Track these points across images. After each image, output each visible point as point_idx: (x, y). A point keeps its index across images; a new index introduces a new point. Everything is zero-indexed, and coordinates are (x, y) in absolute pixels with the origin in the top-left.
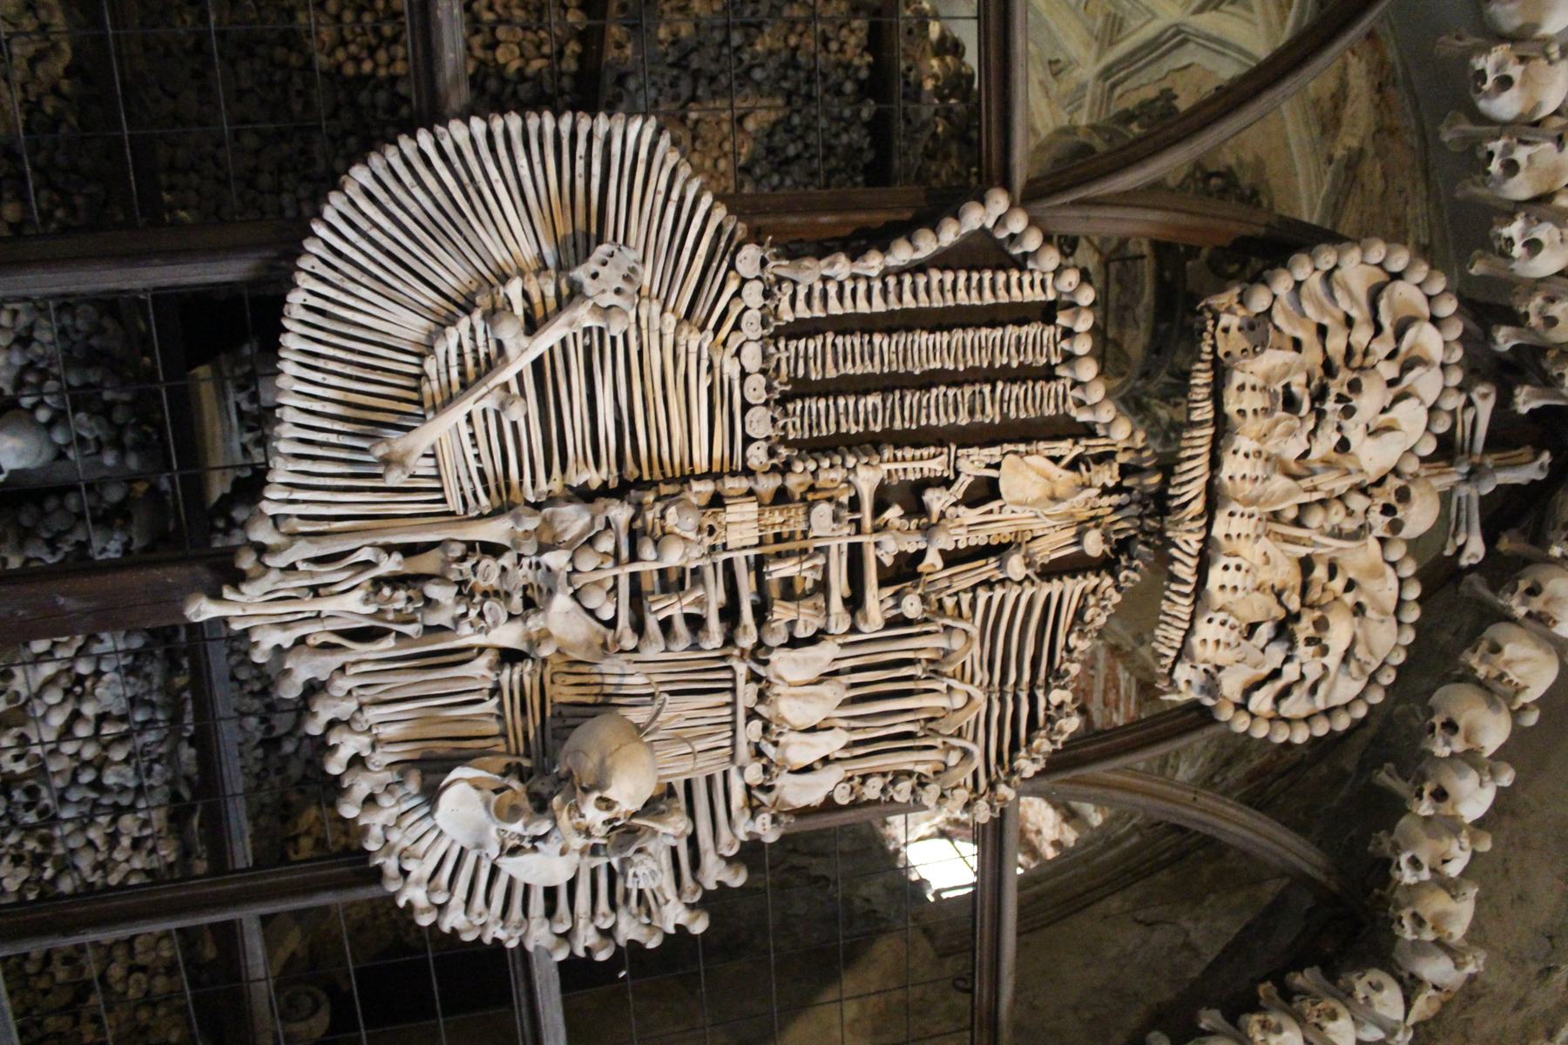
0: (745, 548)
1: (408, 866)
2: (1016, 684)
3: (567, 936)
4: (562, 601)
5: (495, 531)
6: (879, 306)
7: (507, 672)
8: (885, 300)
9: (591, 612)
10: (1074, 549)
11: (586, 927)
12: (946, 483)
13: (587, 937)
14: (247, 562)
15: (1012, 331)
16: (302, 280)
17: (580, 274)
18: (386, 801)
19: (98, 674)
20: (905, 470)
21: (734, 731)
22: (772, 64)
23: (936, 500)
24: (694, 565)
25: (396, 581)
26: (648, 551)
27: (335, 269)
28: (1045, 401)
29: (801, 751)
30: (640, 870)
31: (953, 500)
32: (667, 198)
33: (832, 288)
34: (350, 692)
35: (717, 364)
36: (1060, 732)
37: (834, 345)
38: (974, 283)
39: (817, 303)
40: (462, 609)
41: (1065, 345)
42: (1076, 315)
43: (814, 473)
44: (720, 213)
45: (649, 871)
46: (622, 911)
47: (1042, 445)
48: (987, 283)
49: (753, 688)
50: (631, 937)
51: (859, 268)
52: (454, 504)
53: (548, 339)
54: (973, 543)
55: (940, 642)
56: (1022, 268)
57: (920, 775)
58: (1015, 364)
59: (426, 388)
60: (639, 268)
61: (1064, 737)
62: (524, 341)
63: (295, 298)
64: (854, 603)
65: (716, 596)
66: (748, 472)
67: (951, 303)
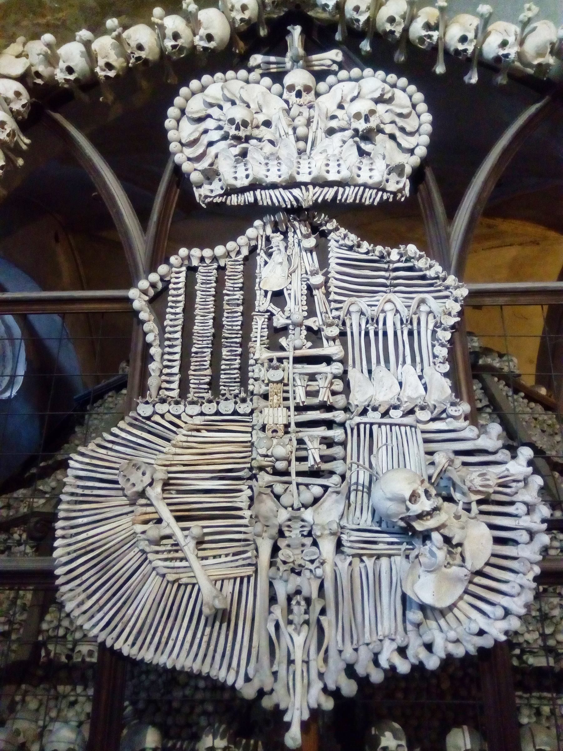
0: (289, 416)
2: (387, 278)
3: (532, 534)
6: (178, 349)
7: (345, 549)
8: (176, 346)
9: (316, 500)
10: (314, 254)
11: (525, 521)
12: (272, 315)
13: (534, 523)
16: (117, 647)
20: (262, 336)
21: (396, 425)
23: (279, 321)
24: (295, 442)
26: (281, 465)
27: (116, 626)
28: (235, 269)
30: (477, 482)
31: (281, 313)
32: (111, 449)
33: (166, 371)
34: (356, 650)
35: (195, 427)
36: (416, 253)
37: (194, 370)
38: (174, 305)
39: (172, 379)
40: (307, 573)
41: (208, 261)
42: (193, 256)
43: (256, 380)
44: (122, 424)
46: (514, 499)
47: (257, 271)
48: (174, 299)
49: (370, 413)
50: (535, 493)
51: (157, 358)
54: (305, 303)
55: (355, 317)
56: (169, 282)
57: (435, 326)
58: (214, 285)
59: (183, 581)
60: (134, 462)
61: (418, 251)
62: (164, 524)
63: (125, 652)
64: (328, 360)
67: (181, 316)
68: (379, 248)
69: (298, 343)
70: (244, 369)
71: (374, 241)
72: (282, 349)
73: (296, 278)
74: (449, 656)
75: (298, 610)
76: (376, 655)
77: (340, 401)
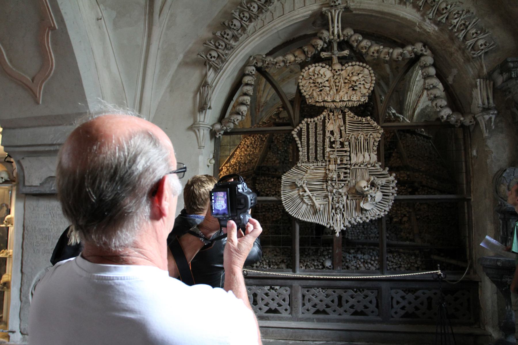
1: (377, 214)
3: (393, 194)
4: (340, 190)
5: (330, 198)
6: (306, 148)
9: (342, 187)
12: (330, 138)
14: (332, 228)
15: (310, 130)
17: (299, 186)
18: (367, 216)
19: (364, 259)
22: (284, 146)
25: (336, 211)
26: (334, 179)
28: (320, 124)
29: (367, 158)
30: (380, 183)
44: (294, 168)
45: (383, 181)
52: (327, 203)
53: (307, 189)
55: (353, 139)
63: (300, 219)
64: (346, 151)
65: (344, 170)
66: (326, 165)
68: (360, 118)
69: (338, 146)
70: (324, 153)
71: (358, 116)
72: (333, 148)
73: (336, 126)
74: (371, 220)
75: (338, 211)
76: (355, 220)
77: (349, 162)
